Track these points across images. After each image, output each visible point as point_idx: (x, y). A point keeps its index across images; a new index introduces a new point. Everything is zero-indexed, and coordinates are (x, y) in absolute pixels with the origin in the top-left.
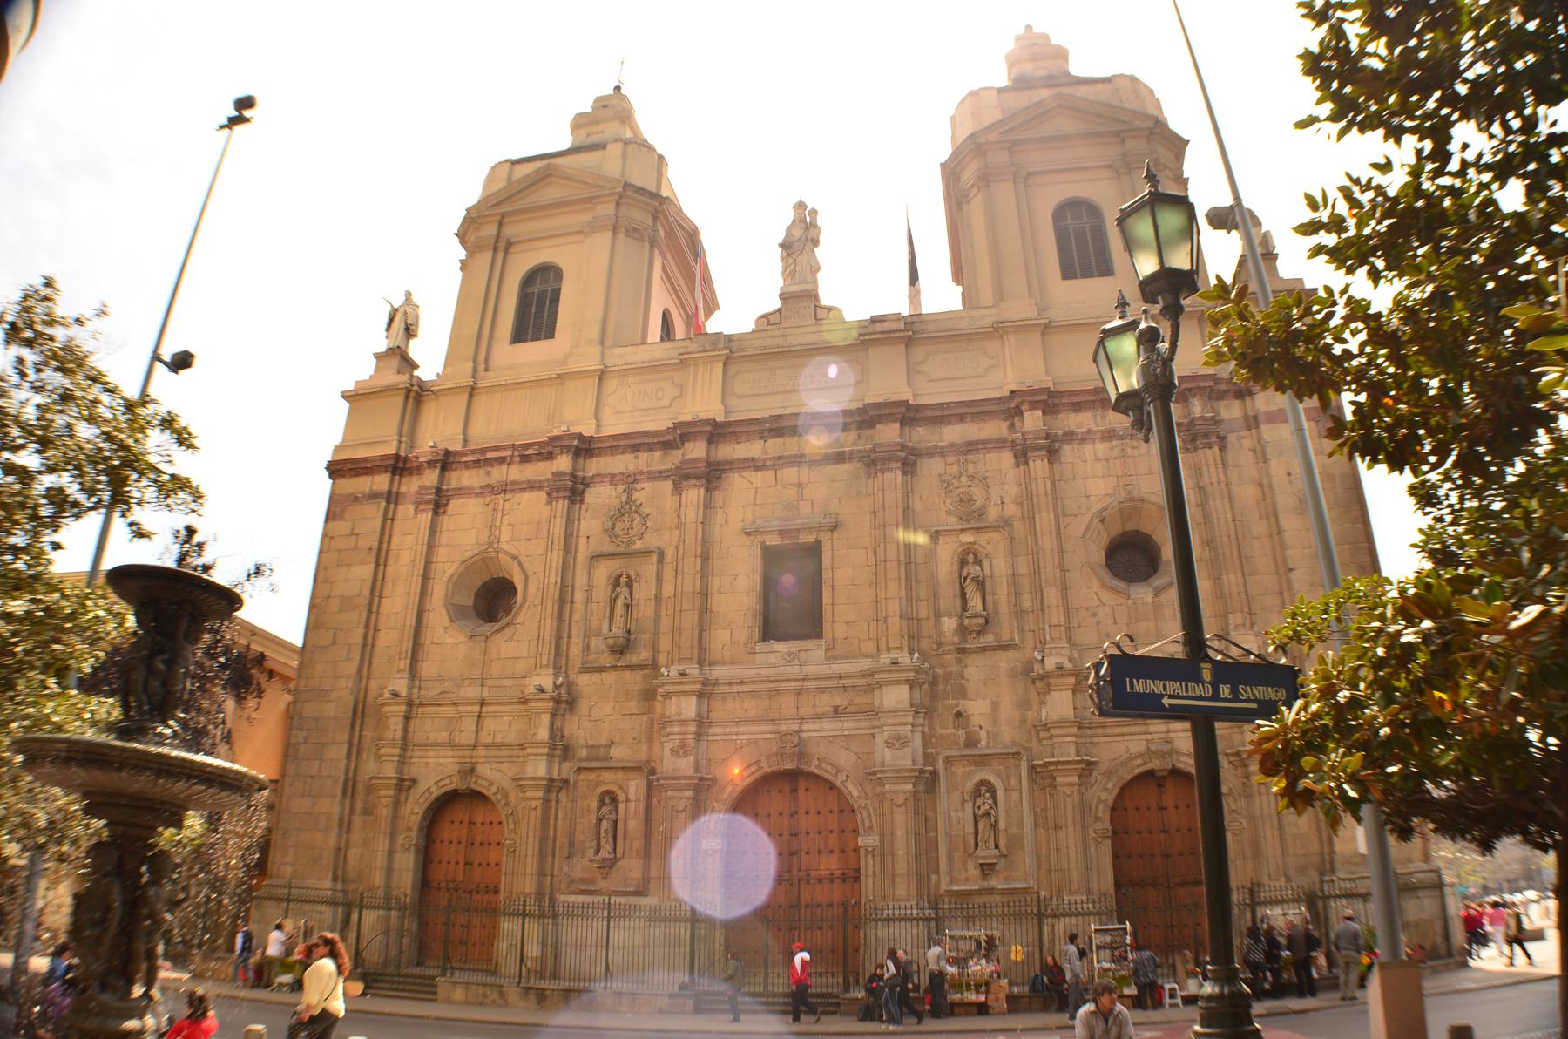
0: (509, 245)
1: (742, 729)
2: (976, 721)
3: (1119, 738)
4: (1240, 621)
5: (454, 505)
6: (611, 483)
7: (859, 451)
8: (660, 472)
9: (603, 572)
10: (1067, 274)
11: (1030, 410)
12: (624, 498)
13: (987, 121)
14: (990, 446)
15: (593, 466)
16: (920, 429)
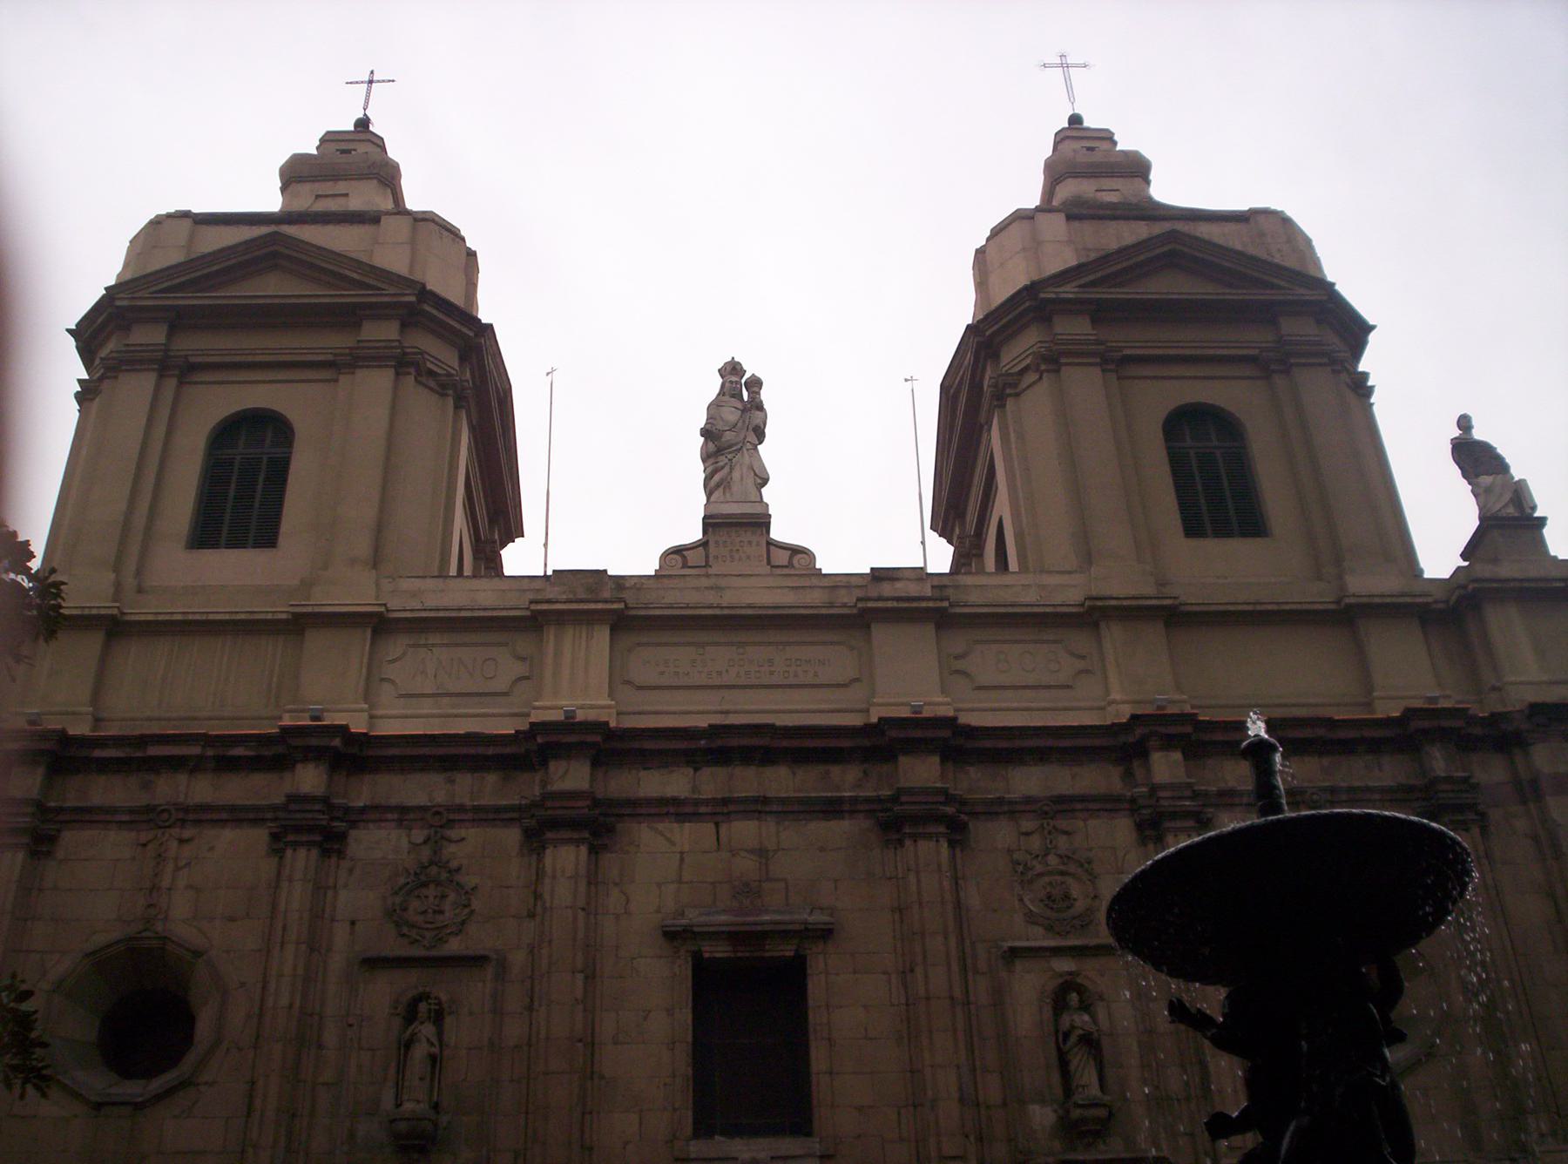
5: (70, 838)
6: (400, 823)
7: (868, 800)
8: (498, 810)
9: (382, 993)
10: (1193, 529)
11: (1161, 749)
12: (426, 853)
13: (1053, 266)
15: (364, 791)
16: (972, 770)
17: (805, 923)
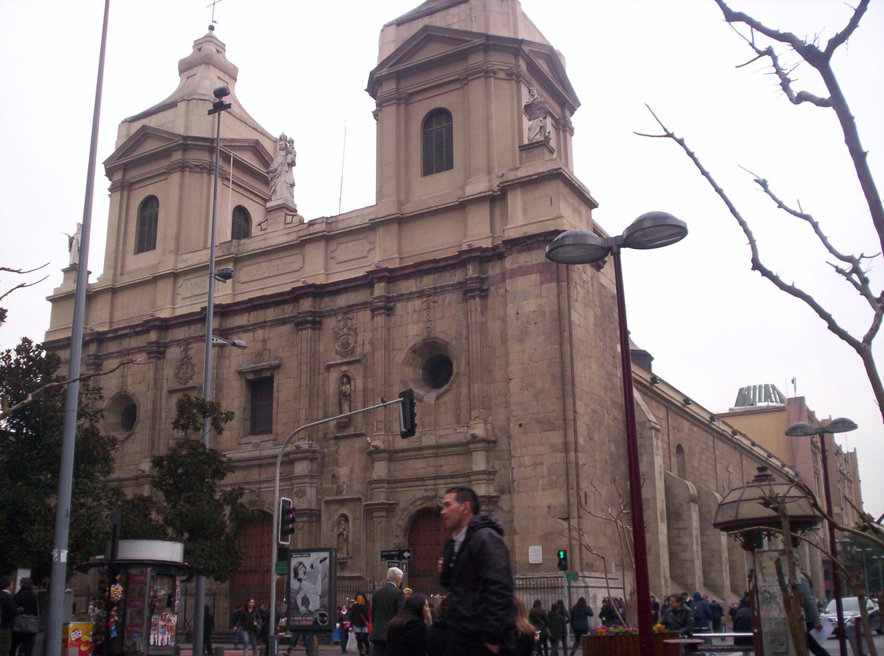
3: (410, 489)
9: (174, 400)
11: (377, 283)
14: (360, 307)
17: (270, 365)
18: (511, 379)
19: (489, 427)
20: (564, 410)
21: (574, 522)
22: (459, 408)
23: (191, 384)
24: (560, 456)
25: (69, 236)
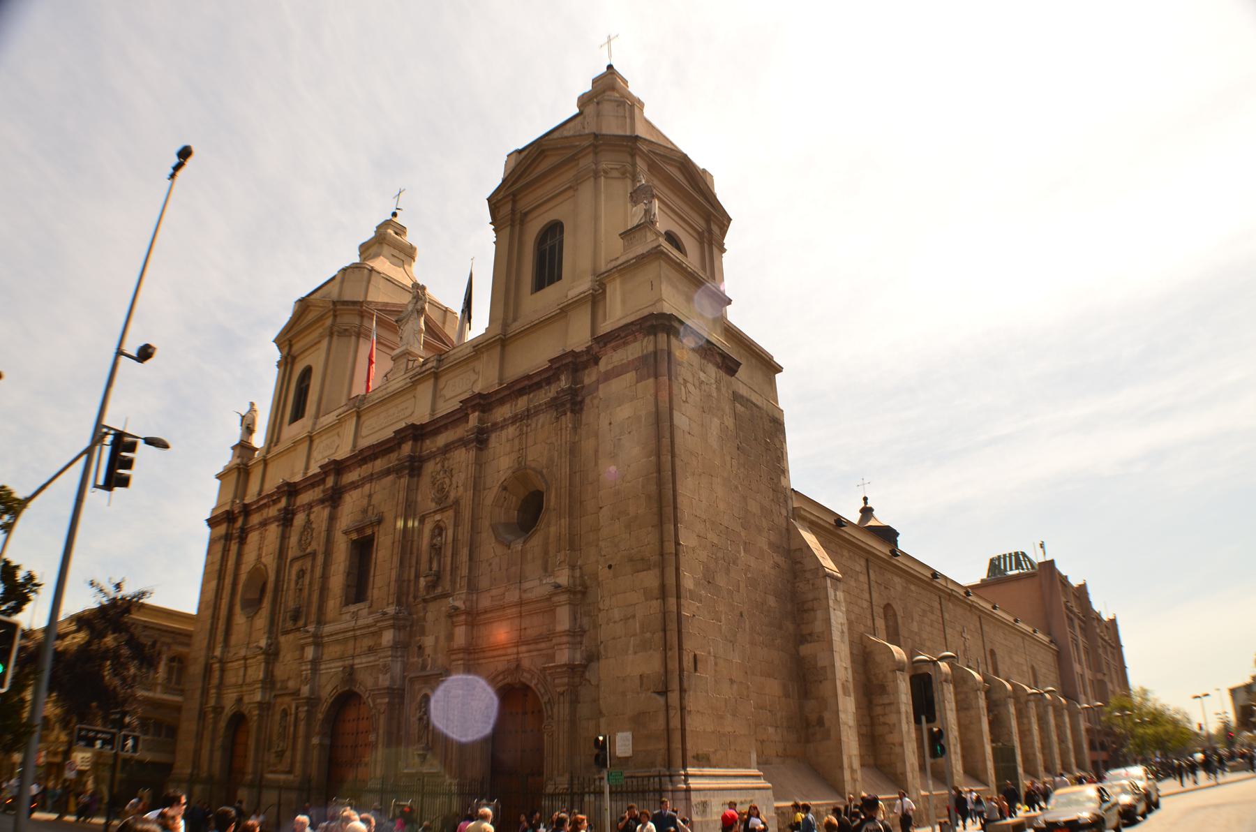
0: (294, 359)
1: (332, 665)
2: (428, 651)
3: (492, 660)
4: (562, 559)
9: (296, 567)
14: (456, 445)
18: (601, 508)
19: (577, 573)
20: (662, 542)
21: (674, 697)
22: (546, 552)
23: (309, 550)
24: (656, 604)
25: (241, 415)
